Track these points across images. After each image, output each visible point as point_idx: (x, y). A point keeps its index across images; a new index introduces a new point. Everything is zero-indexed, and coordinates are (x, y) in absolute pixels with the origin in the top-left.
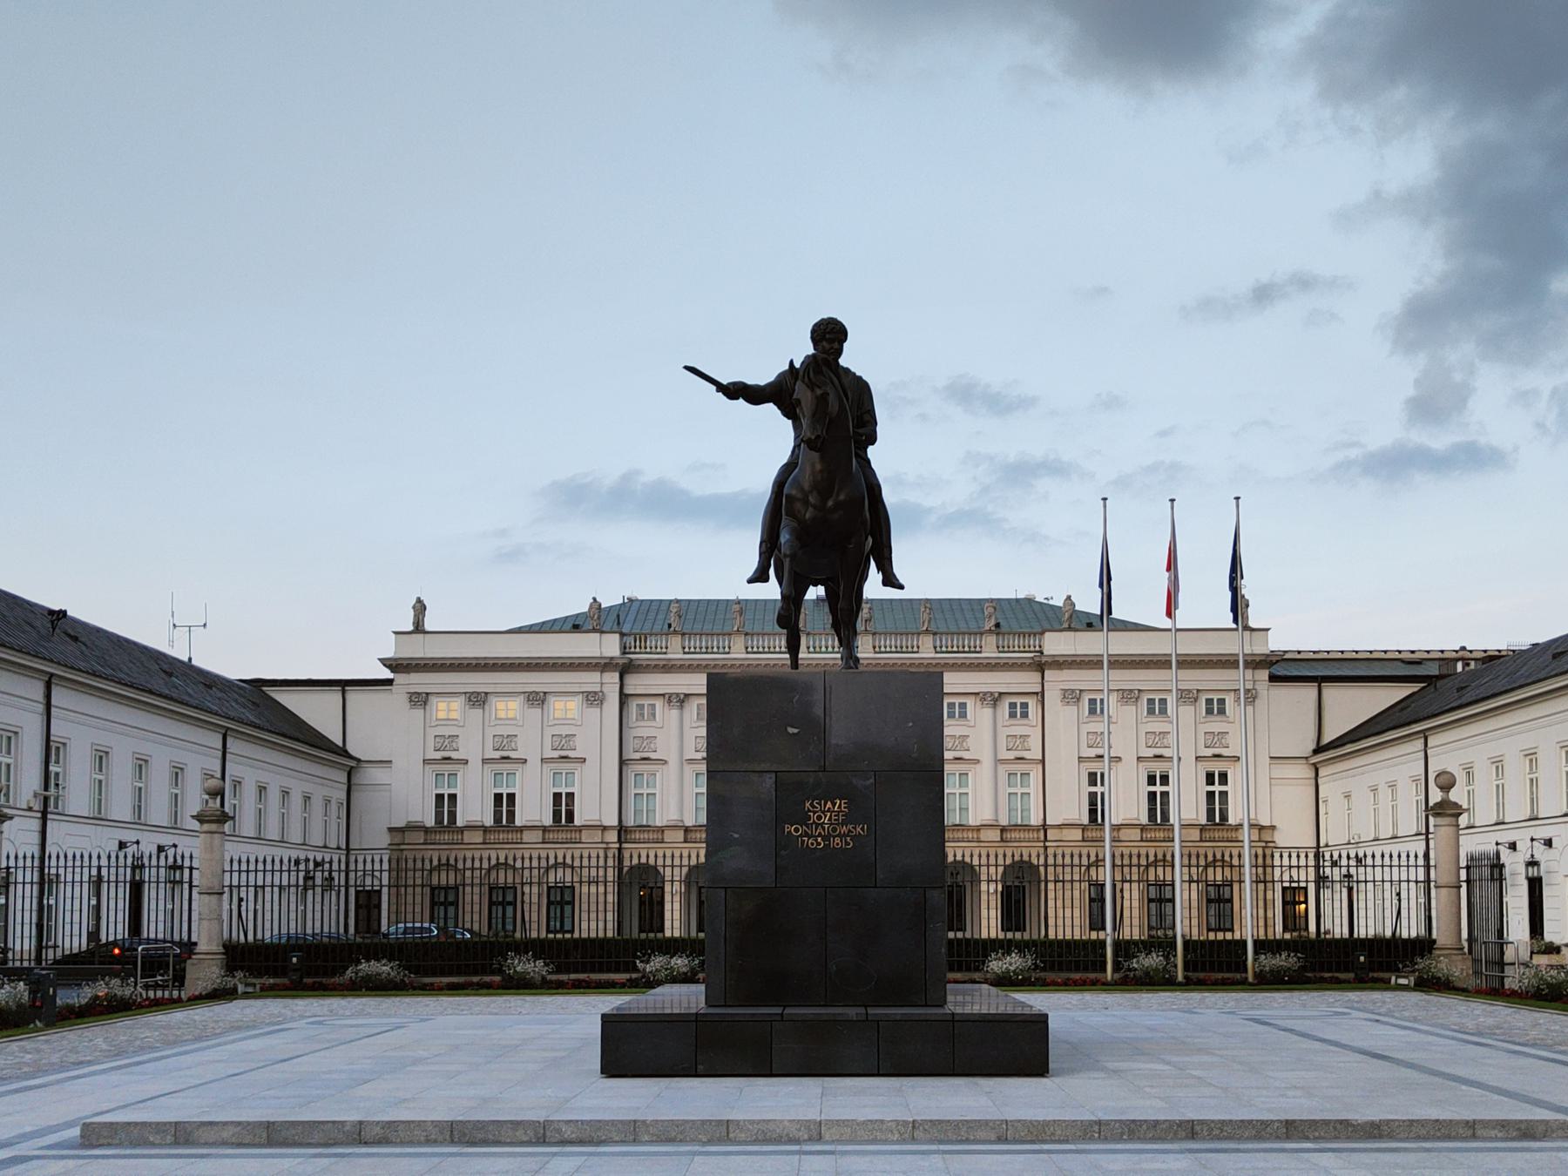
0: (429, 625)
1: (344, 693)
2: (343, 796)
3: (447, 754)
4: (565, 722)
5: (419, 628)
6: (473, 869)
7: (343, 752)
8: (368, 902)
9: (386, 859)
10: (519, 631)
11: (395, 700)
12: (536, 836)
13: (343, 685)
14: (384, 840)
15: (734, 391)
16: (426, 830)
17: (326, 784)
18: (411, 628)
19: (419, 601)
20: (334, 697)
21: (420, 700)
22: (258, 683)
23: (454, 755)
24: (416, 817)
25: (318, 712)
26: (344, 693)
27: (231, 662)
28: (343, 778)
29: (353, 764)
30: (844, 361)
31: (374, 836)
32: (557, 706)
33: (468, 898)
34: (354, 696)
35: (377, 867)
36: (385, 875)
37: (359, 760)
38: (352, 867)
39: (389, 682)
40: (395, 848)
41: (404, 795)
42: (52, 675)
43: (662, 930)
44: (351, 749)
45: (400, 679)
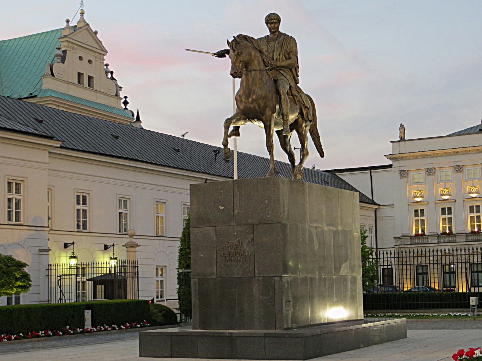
0: (406, 138)
1: (371, 173)
5: (402, 139)
11: (394, 173)
14: (392, 243)
15: (221, 54)
16: (411, 237)
18: (399, 139)
19: (402, 125)
21: (404, 174)
26: (371, 173)
28: (373, 214)
29: (376, 207)
30: (280, 29)
31: (387, 241)
35: (389, 256)
37: (379, 205)
39: (390, 166)
42: (207, 179)
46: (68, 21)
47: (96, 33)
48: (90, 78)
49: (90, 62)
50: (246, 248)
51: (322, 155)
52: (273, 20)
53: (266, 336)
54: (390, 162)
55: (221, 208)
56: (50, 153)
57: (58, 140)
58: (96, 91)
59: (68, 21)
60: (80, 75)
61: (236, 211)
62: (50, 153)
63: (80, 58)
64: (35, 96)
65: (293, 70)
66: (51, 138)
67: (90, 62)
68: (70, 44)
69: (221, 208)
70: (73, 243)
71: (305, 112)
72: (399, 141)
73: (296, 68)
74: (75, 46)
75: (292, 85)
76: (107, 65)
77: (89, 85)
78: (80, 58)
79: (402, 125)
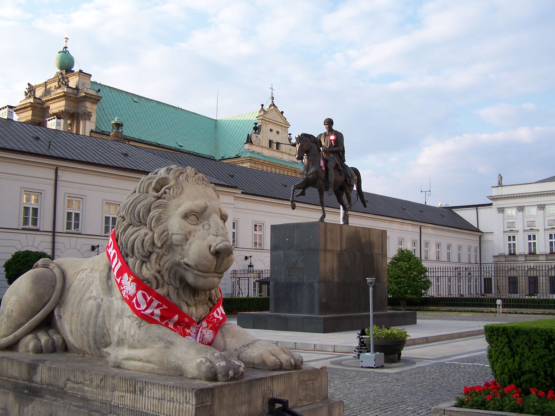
1: (477, 209)
2: (478, 245)
3: (511, 229)
4: (532, 216)
6: (542, 270)
7: (478, 230)
8: (488, 281)
9: (493, 267)
10: (540, 182)
12: (544, 258)
13: (477, 206)
14: (491, 260)
16: (505, 256)
17: (471, 240)
20: (473, 211)
21: (501, 210)
22: (450, 208)
23: (514, 229)
24: (502, 252)
25: (468, 216)
26: (477, 209)
27: (436, 202)
28: (478, 239)
29: (480, 234)
31: (488, 259)
32: (509, 212)
33: (521, 280)
34: (481, 210)
36: (493, 272)
37: (483, 232)
38: (482, 269)
39: (491, 204)
40: (496, 263)
41: (498, 244)
43: (491, 293)
44: (481, 229)
45: (494, 203)
46: (262, 105)
47: (282, 112)
48: (278, 144)
49: (278, 132)
50: (300, 264)
51: (365, 206)
52: (329, 123)
53: (304, 317)
54: (490, 202)
55: (287, 240)
56: (235, 197)
57: (240, 189)
58: (282, 152)
59: (262, 105)
60: (271, 142)
61: (295, 242)
62: (235, 197)
63: (271, 130)
64: (240, 157)
65: (341, 153)
66: (235, 187)
67: (278, 132)
68: (263, 121)
69: (287, 240)
70: (251, 257)
71: (348, 180)
72: (497, 186)
73: (343, 152)
74: (267, 122)
75: (338, 163)
76: (290, 134)
77: (277, 148)
78: (271, 130)
79: (500, 175)
